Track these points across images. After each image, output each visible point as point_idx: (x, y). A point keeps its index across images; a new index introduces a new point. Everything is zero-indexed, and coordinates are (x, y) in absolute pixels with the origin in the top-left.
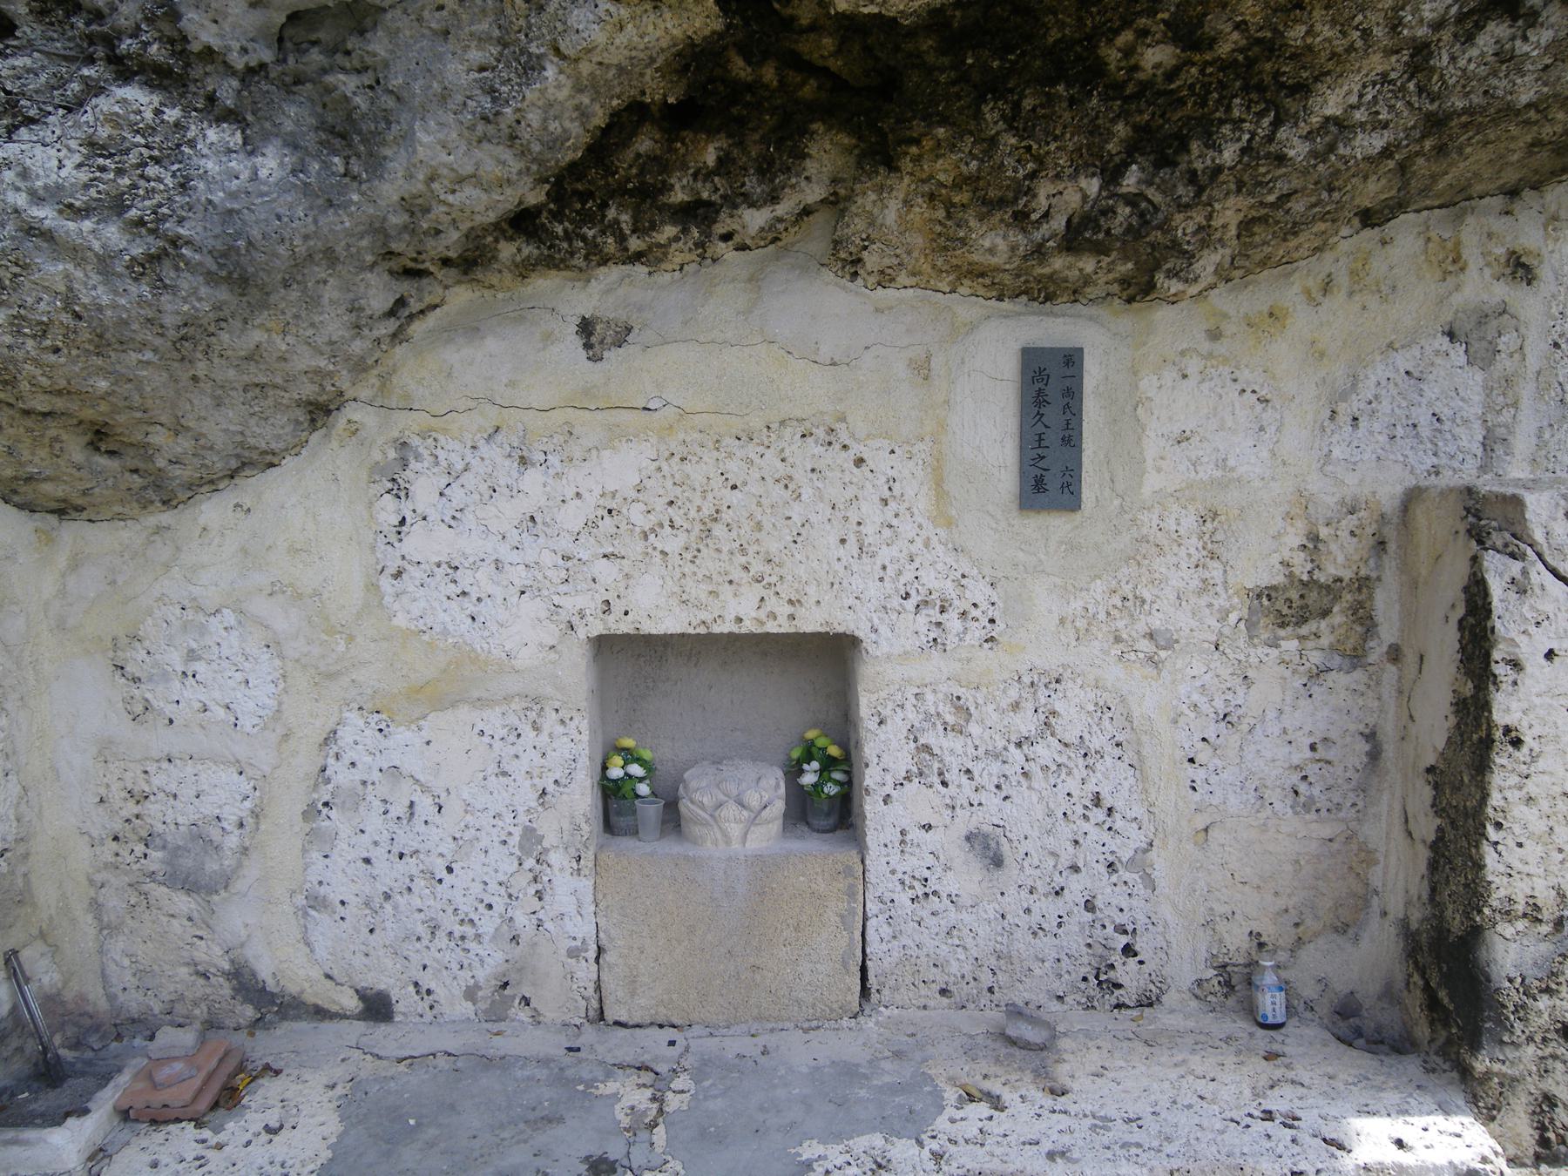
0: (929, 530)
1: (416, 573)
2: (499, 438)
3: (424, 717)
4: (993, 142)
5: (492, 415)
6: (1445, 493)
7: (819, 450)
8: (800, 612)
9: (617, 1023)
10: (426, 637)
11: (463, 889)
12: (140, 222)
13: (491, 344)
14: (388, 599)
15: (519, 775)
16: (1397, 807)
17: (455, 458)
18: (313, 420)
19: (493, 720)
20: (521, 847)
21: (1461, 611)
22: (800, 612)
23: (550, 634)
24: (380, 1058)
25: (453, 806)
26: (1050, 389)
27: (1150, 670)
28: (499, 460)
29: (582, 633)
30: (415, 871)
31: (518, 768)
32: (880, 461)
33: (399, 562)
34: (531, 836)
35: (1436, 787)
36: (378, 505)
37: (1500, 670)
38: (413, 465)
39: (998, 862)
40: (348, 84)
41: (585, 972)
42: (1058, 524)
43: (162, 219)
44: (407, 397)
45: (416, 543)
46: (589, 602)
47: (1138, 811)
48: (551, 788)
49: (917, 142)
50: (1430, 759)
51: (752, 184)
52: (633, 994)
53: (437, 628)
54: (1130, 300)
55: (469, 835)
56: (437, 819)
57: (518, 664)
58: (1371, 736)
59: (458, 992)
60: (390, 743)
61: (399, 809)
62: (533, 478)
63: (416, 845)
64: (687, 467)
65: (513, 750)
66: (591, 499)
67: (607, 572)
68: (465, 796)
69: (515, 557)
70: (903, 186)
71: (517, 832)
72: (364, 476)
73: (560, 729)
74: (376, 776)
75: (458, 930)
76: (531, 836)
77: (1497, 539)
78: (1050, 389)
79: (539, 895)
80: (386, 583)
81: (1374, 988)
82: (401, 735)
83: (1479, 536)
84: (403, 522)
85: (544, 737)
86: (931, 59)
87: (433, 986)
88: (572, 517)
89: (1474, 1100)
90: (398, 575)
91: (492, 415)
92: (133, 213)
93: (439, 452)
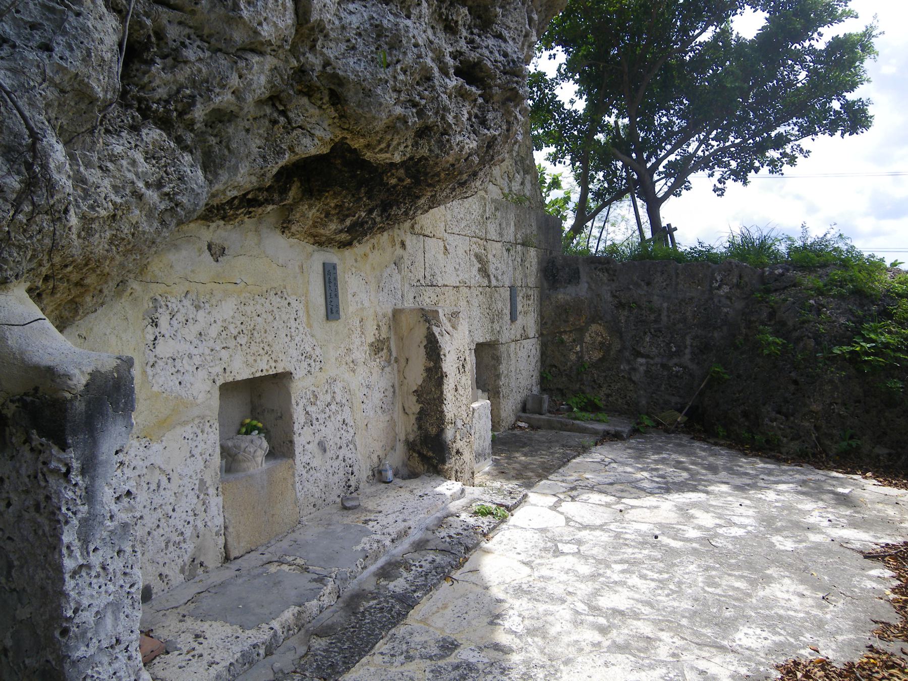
0: (307, 329)
1: (161, 363)
2: (189, 296)
3: (163, 436)
4: (361, 199)
5: (186, 286)
6: (412, 310)
7: (279, 300)
8: (278, 365)
9: (235, 558)
10: (164, 395)
11: (178, 520)
12: (167, 194)
13: (184, 253)
14: (150, 378)
15: (197, 456)
16: (401, 407)
17: (174, 306)
18: (570, 281)
19: (188, 431)
20: (199, 489)
21: (425, 343)
22: (278, 365)
23: (208, 385)
24: (176, 608)
25: (175, 477)
26: (330, 276)
27: (352, 374)
28: (189, 306)
29: (219, 383)
30: (161, 516)
31: (196, 452)
32: (294, 304)
33: (154, 359)
34: (202, 482)
35: (418, 396)
36: (146, 330)
37: (442, 357)
38: (160, 310)
39: (325, 451)
40: (213, 141)
41: (221, 541)
42: (334, 324)
43: (175, 194)
44: (155, 276)
45: (160, 349)
46: (219, 369)
47: (352, 423)
48: (208, 458)
49: (328, 192)
50: (415, 388)
51: (276, 197)
52: (239, 543)
53: (169, 390)
54: (339, 248)
55: (180, 490)
56: (169, 486)
57: (199, 401)
58: (393, 386)
59: (177, 571)
60: (150, 452)
61: (153, 486)
62: (201, 313)
63: (161, 502)
64: (246, 307)
65: (195, 444)
66: (219, 323)
67: (224, 354)
68: (179, 471)
69: (195, 351)
70: (319, 205)
71: (197, 482)
72: (141, 317)
73: (210, 430)
74: (145, 471)
75: (177, 539)
76: (202, 482)
77: (433, 322)
78: (330, 276)
79: (205, 511)
80: (149, 369)
81: (400, 464)
82: (156, 447)
83: (427, 321)
84: (155, 339)
85: (205, 435)
86: (339, 167)
87: (168, 573)
88: (214, 331)
89: (445, 477)
90: (153, 365)
91: (186, 286)
92: (166, 190)
93: (168, 303)
